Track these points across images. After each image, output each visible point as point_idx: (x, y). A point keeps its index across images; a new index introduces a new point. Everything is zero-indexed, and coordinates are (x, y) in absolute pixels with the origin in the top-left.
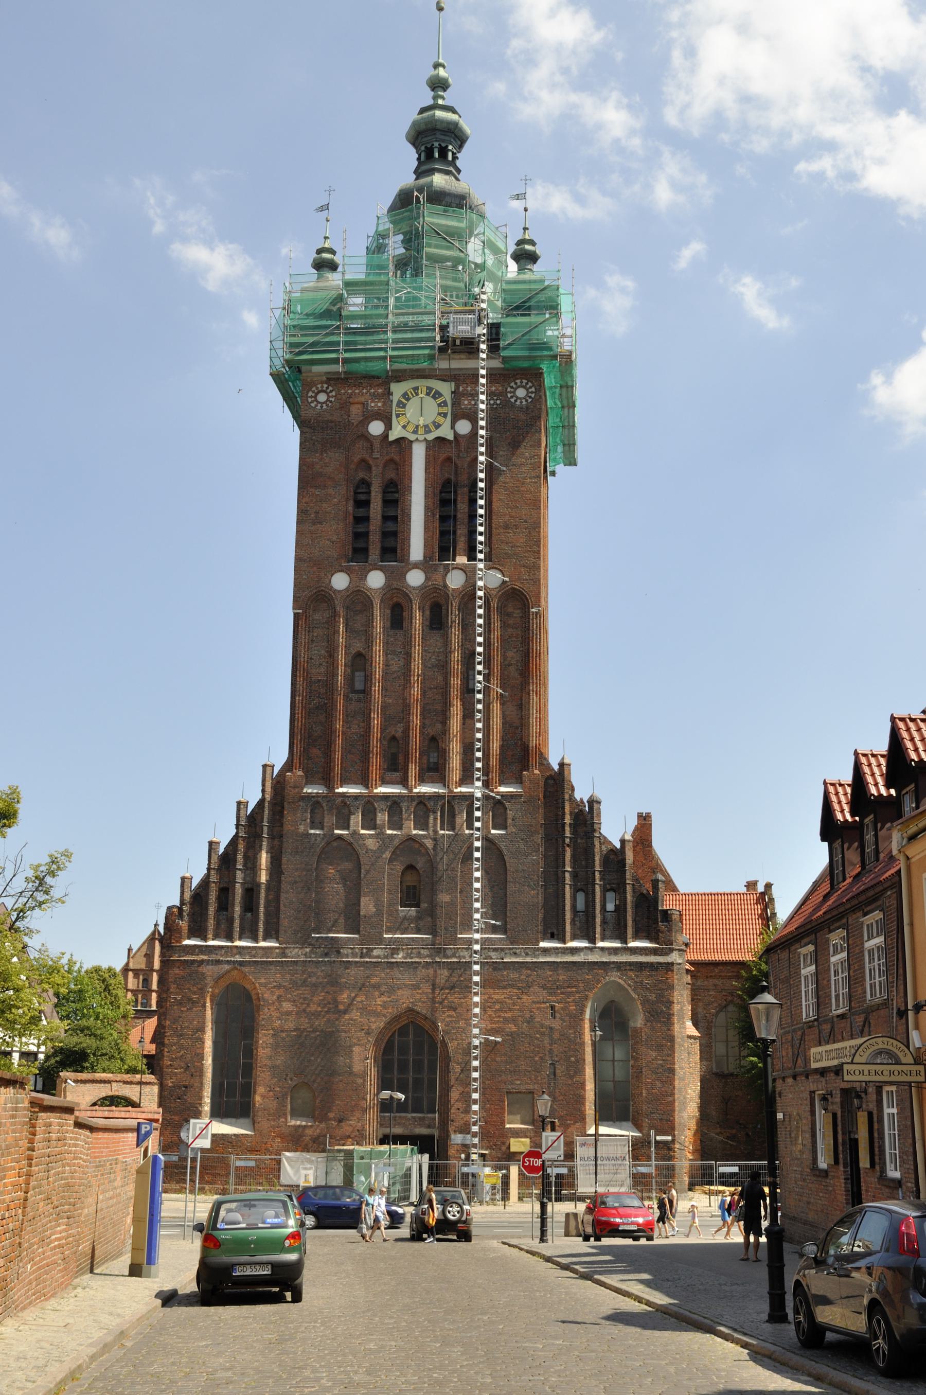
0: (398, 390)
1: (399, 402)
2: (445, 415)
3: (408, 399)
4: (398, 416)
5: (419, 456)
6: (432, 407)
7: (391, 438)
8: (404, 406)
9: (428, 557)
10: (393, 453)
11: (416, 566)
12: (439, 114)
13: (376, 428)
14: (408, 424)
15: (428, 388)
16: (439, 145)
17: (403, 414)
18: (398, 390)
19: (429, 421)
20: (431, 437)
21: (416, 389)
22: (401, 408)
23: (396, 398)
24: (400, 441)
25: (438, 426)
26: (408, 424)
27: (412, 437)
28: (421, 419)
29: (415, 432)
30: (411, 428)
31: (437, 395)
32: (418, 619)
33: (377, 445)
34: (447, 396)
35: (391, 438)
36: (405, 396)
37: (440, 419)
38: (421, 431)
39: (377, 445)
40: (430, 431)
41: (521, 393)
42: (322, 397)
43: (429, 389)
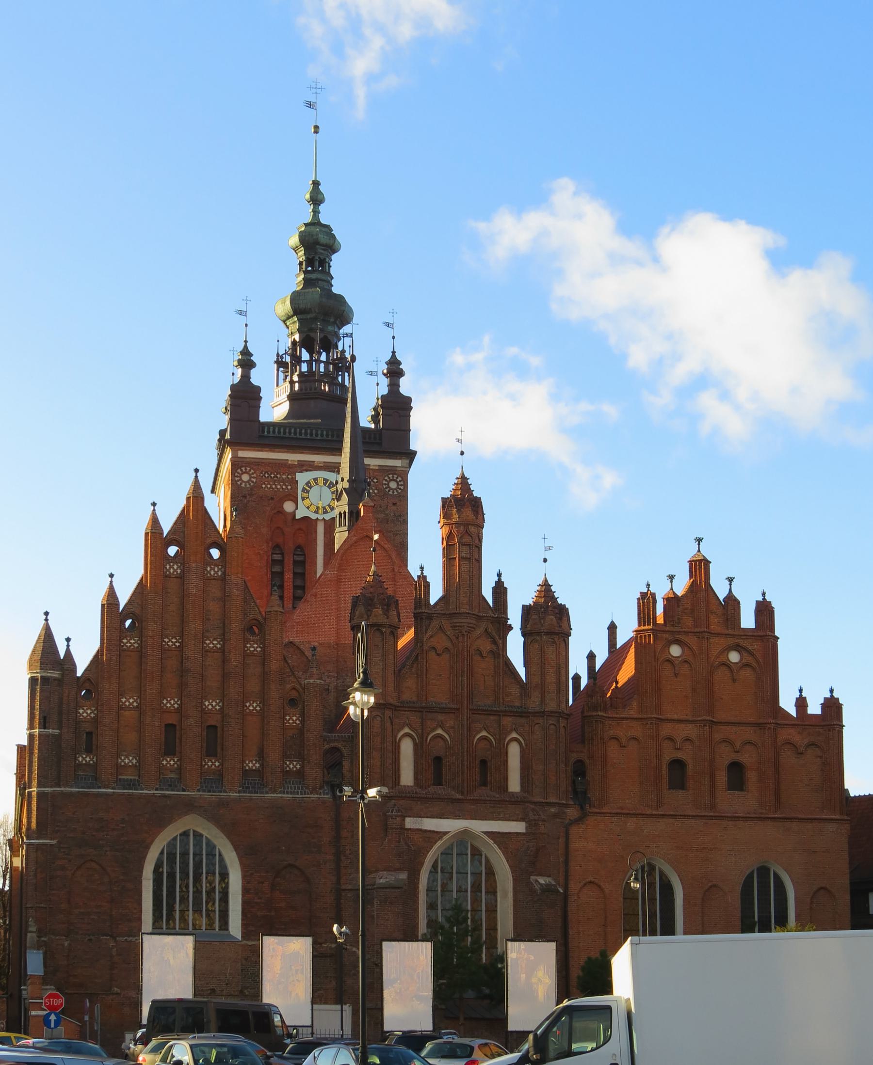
0: (302, 478)
1: (304, 490)
3: (311, 487)
4: (303, 499)
7: (297, 517)
8: (308, 492)
14: (311, 505)
15: (324, 479)
16: (319, 258)
17: (307, 498)
18: (302, 478)
19: (326, 504)
21: (316, 480)
22: (306, 493)
23: (301, 485)
26: (311, 505)
27: (314, 516)
28: (320, 502)
29: (316, 512)
30: (313, 508)
35: (297, 517)
36: (308, 483)
38: (321, 511)
40: (325, 512)
41: (393, 485)
43: (326, 480)
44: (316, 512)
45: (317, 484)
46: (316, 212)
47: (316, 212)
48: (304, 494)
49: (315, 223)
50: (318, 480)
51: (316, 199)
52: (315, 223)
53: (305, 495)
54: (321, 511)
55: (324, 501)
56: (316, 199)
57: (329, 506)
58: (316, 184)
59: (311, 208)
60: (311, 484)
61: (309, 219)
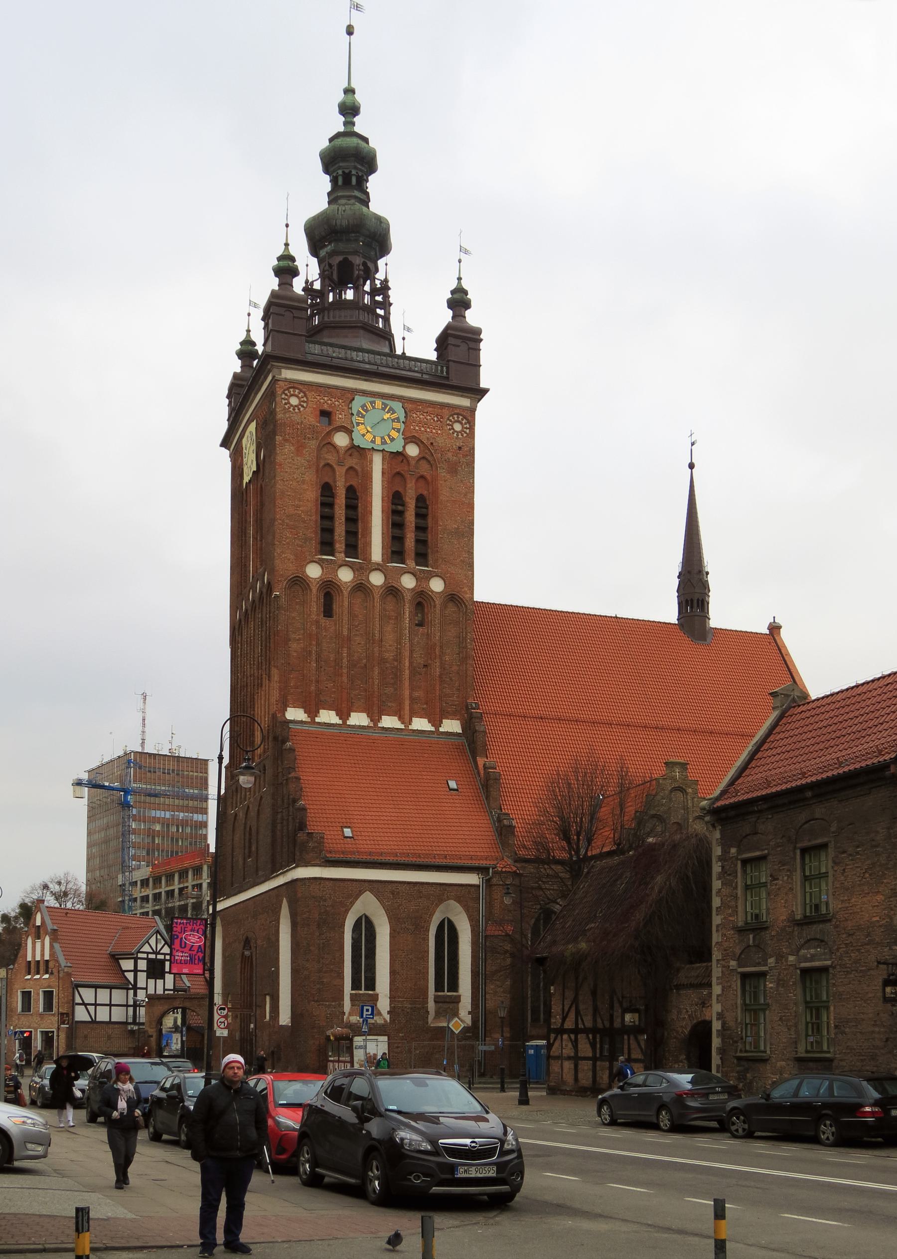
2: (398, 431)
4: (358, 424)
12: (355, 141)
22: (361, 417)
30: (369, 437)
37: (394, 434)
44: (373, 442)
45: (374, 408)
46: (349, 123)
47: (349, 123)
48: (359, 419)
49: (349, 133)
50: (375, 404)
51: (349, 110)
52: (349, 133)
53: (361, 420)
54: (378, 441)
55: (383, 430)
56: (349, 110)
57: (389, 436)
58: (349, 91)
59: (342, 119)
60: (367, 407)
61: (342, 129)
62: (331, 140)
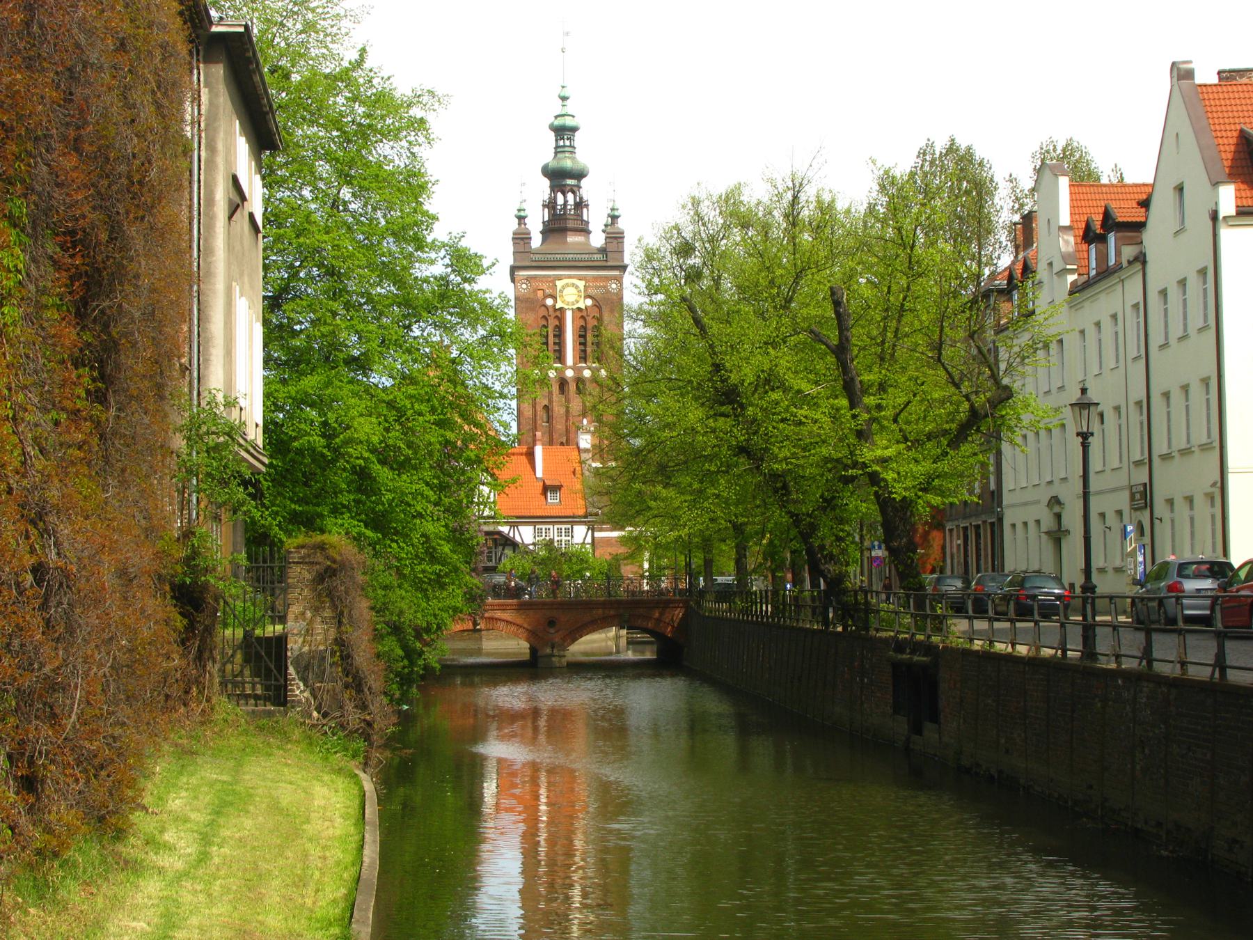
0: (559, 284)
5: (569, 315)
6: (573, 290)
9: (575, 364)
10: (558, 314)
11: (570, 368)
13: (549, 302)
18: (559, 284)
20: (574, 307)
23: (559, 288)
24: (561, 309)
25: (577, 302)
27: (566, 307)
31: (577, 287)
32: (572, 387)
33: (551, 310)
34: (582, 288)
39: (551, 310)
41: (614, 286)
42: (524, 286)
43: (573, 285)
62: (556, 117)
